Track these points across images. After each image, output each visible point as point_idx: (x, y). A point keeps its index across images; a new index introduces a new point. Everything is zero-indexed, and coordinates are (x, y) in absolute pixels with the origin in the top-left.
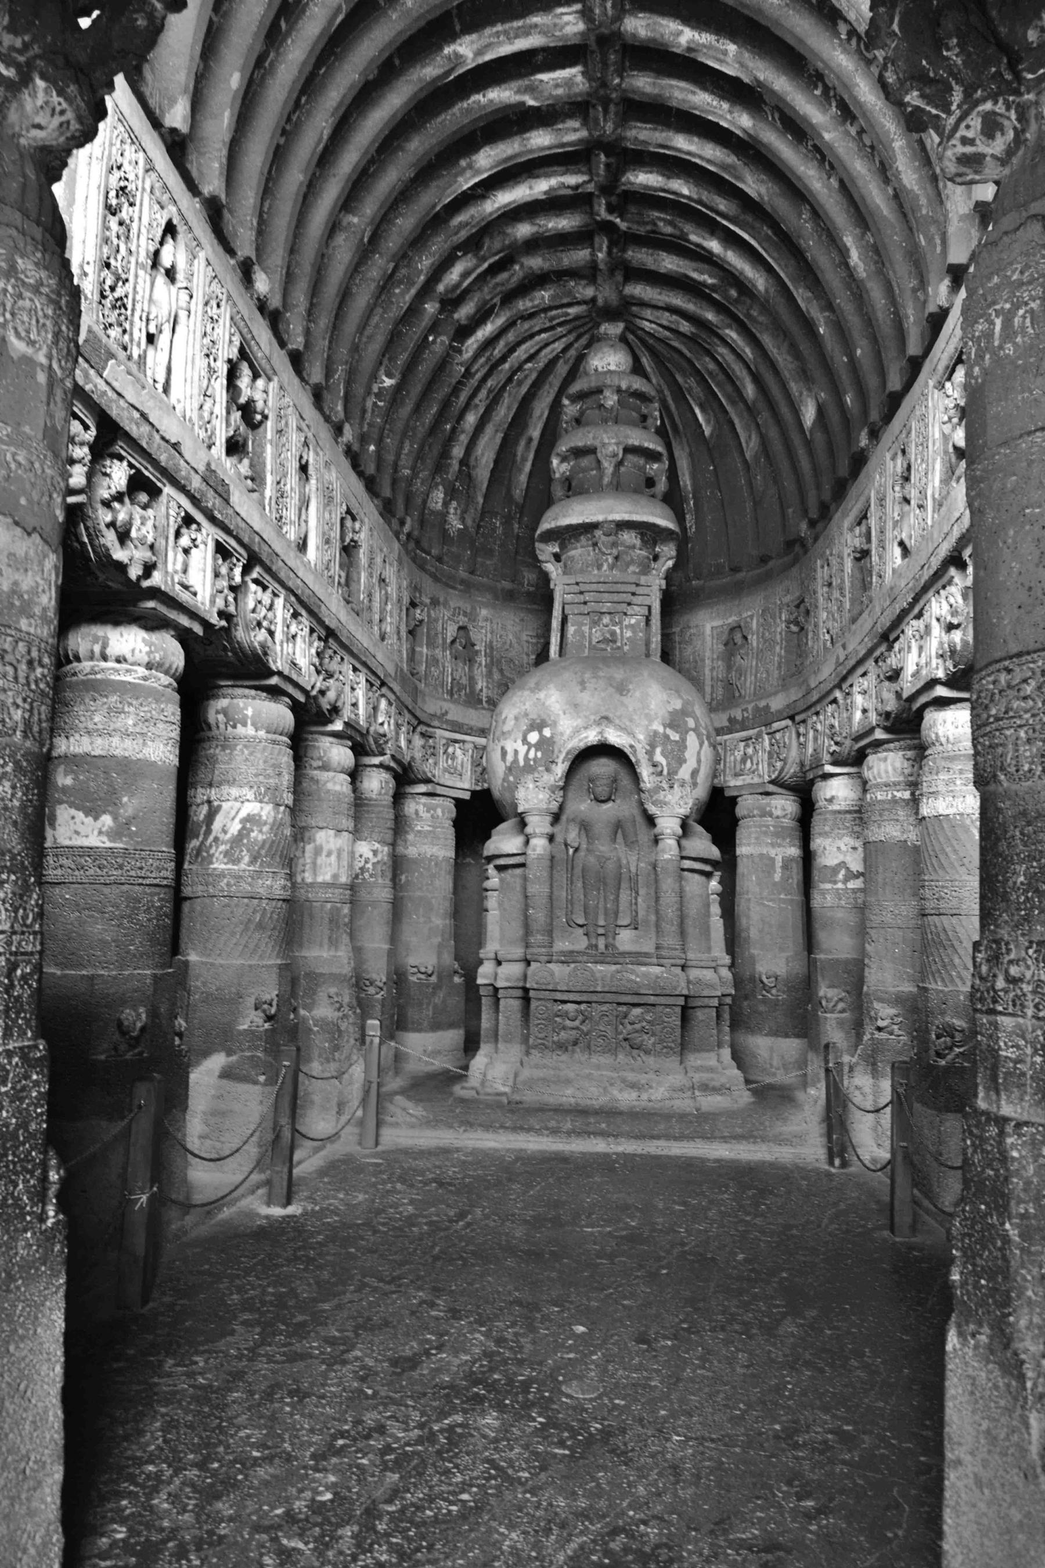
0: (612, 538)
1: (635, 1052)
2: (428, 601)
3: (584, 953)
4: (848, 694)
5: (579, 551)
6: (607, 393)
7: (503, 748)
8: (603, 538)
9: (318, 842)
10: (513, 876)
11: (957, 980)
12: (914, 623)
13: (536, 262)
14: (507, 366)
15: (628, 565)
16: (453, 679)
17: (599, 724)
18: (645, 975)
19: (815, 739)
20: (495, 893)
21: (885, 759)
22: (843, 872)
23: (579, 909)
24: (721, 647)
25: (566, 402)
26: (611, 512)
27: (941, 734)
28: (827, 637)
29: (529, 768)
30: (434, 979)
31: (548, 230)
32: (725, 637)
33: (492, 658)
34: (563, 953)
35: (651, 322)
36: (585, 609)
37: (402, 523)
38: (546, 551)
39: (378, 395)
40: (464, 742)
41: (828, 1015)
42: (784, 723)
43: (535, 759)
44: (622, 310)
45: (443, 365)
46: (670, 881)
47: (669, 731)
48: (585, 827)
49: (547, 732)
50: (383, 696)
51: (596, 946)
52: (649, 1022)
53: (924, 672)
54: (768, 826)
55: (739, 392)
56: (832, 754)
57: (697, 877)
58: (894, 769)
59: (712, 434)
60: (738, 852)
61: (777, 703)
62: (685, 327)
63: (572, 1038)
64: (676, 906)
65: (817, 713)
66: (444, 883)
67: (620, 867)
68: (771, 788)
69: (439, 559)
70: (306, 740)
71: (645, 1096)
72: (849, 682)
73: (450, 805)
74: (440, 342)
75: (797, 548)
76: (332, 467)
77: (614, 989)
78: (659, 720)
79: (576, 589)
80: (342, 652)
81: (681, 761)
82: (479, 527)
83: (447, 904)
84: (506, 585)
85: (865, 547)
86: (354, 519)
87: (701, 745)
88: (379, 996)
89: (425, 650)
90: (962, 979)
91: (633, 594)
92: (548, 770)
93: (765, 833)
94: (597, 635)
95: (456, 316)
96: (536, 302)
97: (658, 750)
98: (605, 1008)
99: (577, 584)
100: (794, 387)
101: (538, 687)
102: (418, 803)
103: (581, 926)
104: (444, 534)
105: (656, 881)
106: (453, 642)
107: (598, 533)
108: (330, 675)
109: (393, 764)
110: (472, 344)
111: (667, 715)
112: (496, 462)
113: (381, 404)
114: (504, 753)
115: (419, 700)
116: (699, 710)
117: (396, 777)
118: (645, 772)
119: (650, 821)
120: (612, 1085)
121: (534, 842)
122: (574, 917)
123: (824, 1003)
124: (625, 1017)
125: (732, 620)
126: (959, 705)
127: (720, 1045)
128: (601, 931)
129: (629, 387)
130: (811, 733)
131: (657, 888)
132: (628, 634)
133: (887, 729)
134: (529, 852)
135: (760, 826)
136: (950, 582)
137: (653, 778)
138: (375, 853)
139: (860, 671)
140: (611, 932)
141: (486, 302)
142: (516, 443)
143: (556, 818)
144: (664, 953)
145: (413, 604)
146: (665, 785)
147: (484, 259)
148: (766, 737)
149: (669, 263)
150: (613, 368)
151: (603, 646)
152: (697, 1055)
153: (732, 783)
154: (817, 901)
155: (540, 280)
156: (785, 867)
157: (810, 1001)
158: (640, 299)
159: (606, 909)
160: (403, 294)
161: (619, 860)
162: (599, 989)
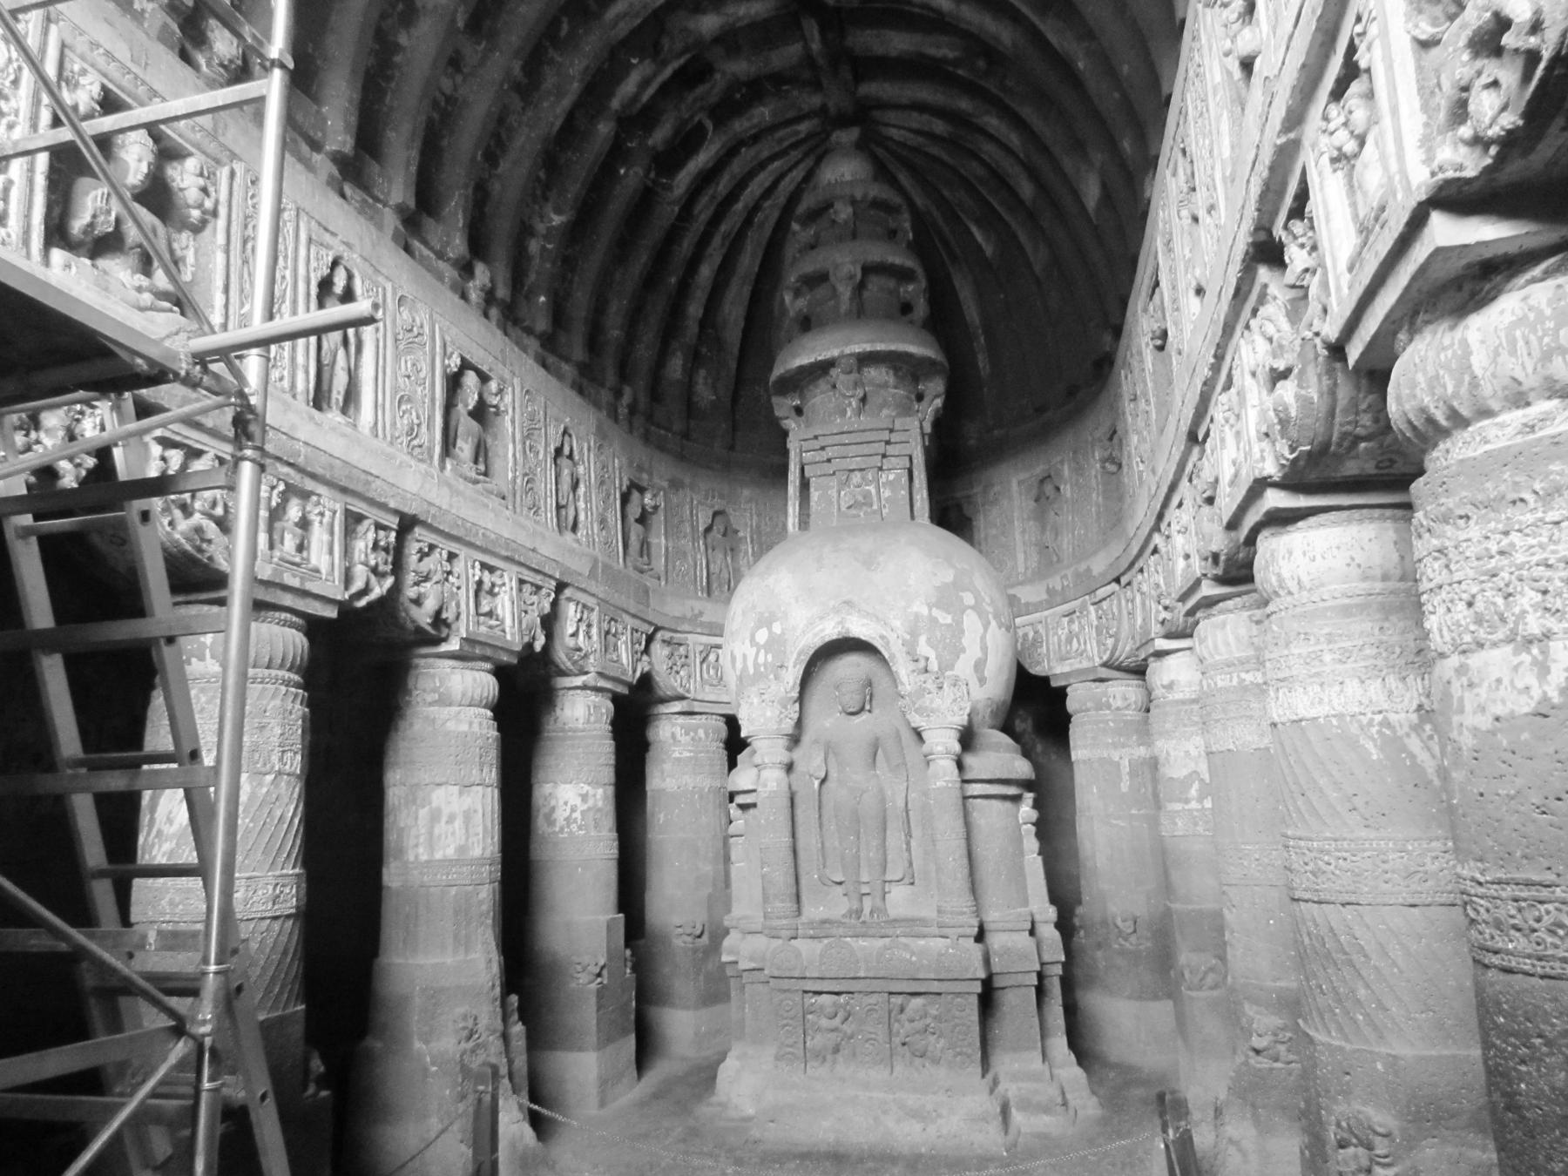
0: (854, 376)
1: (918, 1061)
2: (665, 484)
3: (840, 924)
6: (838, 206)
8: (842, 377)
9: (434, 805)
11: (1367, 1031)
12: (1224, 398)
13: (740, 67)
14: (739, 206)
15: (881, 407)
17: (837, 611)
19: (1143, 604)
21: (1224, 625)
22: (1196, 786)
24: (1032, 504)
25: (795, 226)
26: (847, 345)
27: (1286, 574)
29: (758, 676)
30: (705, 939)
31: (739, 19)
32: (1034, 492)
33: (761, 545)
34: (811, 924)
35: (900, 127)
36: (829, 468)
37: (618, 394)
38: (782, 406)
39: (546, 237)
41: (1194, 994)
43: (765, 665)
44: (862, 115)
47: (935, 612)
49: (777, 628)
50: (569, 599)
52: (935, 1018)
53: (1244, 472)
55: (1013, 192)
58: (1238, 639)
60: (1073, 758)
61: (1099, 564)
62: (939, 127)
65: (1141, 571)
67: (883, 801)
68: (1104, 673)
69: (686, 435)
70: (417, 666)
71: (932, 1130)
74: (631, 176)
76: (419, 305)
79: (816, 444)
80: (448, 546)
86: (484, 378)
87: (986, 626)
90: (1376, 1028)
91: (888, 443)
94: (846, 499)
95: (650, 142)
96: (755, 121)
97: (923, 639)
98: (873, 999)
99: (816, 437)
100: (1068, 163)
102: (674, 725)
103: (840, 883)
104: (690, 408)
106: (708, 530)
107: (834, 372)
108: (426, 579)
110: (684, 179)
112: (750, 318)
113: (549, 246)
115: (653, 601)
117: (616, 699)
118: (903, 668)
120: (885, 1112)
121: (766, 774)
123: (1187, 975)
124: (902, 1010)
125: (1040, 470)
126: (1312, 520)
128: (865, 889)
129: (865, 196)
133: (1222, 580)
136: (1262, 299)
138: (584, 798)
139: (1175, 501)
144: (947, 919)
145: (635, 487)
146: (930, 686)
147: (664, 64)
148: (1092, 608)
149: (899, 43)
150: (848, 177)
151: (853, 511)
153: (1058, 670)
155: (754, 90)
156: (1133, 774)
161: (881, 791)
162: (862, 974)
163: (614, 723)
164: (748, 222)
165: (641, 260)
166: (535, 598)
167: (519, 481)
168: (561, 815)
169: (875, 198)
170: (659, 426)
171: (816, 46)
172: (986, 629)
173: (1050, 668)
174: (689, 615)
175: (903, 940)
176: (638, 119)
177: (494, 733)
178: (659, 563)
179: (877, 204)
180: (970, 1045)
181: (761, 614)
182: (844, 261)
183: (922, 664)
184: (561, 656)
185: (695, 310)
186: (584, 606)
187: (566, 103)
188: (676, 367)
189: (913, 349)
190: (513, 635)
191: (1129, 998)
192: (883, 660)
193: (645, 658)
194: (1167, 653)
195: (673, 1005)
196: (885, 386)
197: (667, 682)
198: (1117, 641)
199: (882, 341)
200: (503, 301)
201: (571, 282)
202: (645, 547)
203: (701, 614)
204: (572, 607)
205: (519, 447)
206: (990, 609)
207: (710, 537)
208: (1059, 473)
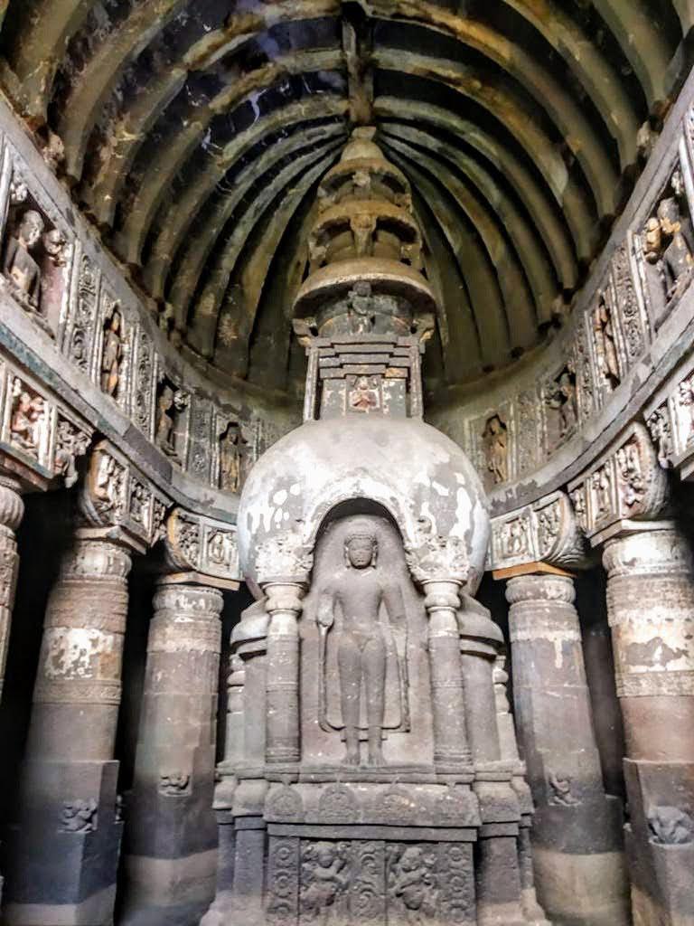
1: (412, 914)
2: (193, 391)
3: (342, 770)
4: (654, 421)
5: (335, 319)
7: (249, 515)
8: (357, 298)
10: (258, 666)
13: (290, 62)
14: (271, 187)
16: (221, 471)
17: (353, 475)
18: (422, 799)
20: (240, 689)
22: (659, 650)
23: (334, 705)
24: (480, 439)
25: (321, 192)
26: (363, 273)
28: (607, 382)
31: (296, 14)
32: (483, 428)
34: (312, 770)
35: (402, 140)
36: (341, 373)
37: (162, 308)
38: (302, 326)
40: (232, 532)
41: (667, 846)
42: (554, 496)
43: (281, 523)
45: (197, 160)
46: (448, 666)
47: (436, 485)
48: (339, 600)
49: (295, 490)
50: (103, 452)
51: (357, 759)
52: (430, 868)
54: (543, 608)
56: (630, 506)
57: (479, 662)
59: (459, 253)
61: (541, 479)
62: (433, 143)
63: (325, 895)
64: (458, 700)
66: (205, 682)
67: (385, 650)
68: (544, 567)
69: (210, 360)
72: (659, 400)
73: (219, 597)
75: (551, 331)
77: (381, 821)
78: (425, 472)
79: (331, 352)
81: (453, 521)
82: (252, 342)
83: (209, 703)
84: (281, 394)
85: (668, 230)
86: (48, 226)
87: (474, 504)
88: (82, 832)
89: (187, 435)
91: (392, 355)
92: (294, 531)
93: (541, 616)
94: (354, 397)
95: (211, 106)
96: (293, 114)
97: (425, 506)
98: (369, 847)
99: (332, 346)
101: (288, 445)
103: (339, 729)
104: (217, 342)
105: (430, 666)
106: (223, 436)
107: (351, 294)
109: (124, 538)
110: (232, 150)
111: (432, 467)
113: (118, 156)
114: (250, 519)
115: (175, 482)
116: (467, 465)
117: (134, 555)
118: (409, 527)
119: (419, 588)
121: (276, 619)
122: (328, 716)
123: (656, 826)
124: (397, 860)
125: (488, 412)
127: (523, 886)
128: (363, 735)
129: (381, 169)
130: (593, 494)
131: (431, 677)
132: (387, 396)
134: (271, 633)
135: (536, 609)
137: (420, 536)
138: (94, 643)
140: (375, 737)
141: (240, 96)
142: (286, 267)
143: (306, 588)
144: (445, 766)
146: (434, 543)
147: (233, 36)
148: (534, 515)
149: (412, 62)
151: (359, 408)
152: (496, 907)
153: (499, 567)
154: (627, 689)
156: (566, 652)
157: (627, 818)
158: (390, 112)
159: (368, 705)
160: (136, 33)
161: (383, 640)
162: (361, 821)
163: (130, 576)
164: (275, 204)
165: (191, 203)
166: (71, 437)
167: (69, 328)
168: (68, 659)
169: (388, 173)
170: (191, 347)
171: (350, 54)
172: (474, 504)
173: (493, 565)
174: (202, 500)
175: (401, 786)
176: (203, 82)
177: (12, 552)
178: (183, 453)
179: (389, 180)
180: (465, 896)
181: (281, 479)
182: (362, 213)
183: (426, 525)
184: (89, 505)
185: (228, 263)
186: (117, 463)
187: (149, 33)
188: (208, 305)
189: (415, 284)
190: (46, 462)
191: (564, 851)
192: (393, 523)
193: (163, 527)
194: (628, 533)
195: (152, 854)
196: (390, 313)
197: (178, 552)
198: (559, 539)
199: (393, 273)
200: (73, 177)
201: (133, 201)
202: (171, 436)
203: (212, 501)
204: (105, 460)
205: (73, 299)
206: (476, 491)
207: (223, 442)
208: (505, 412)
